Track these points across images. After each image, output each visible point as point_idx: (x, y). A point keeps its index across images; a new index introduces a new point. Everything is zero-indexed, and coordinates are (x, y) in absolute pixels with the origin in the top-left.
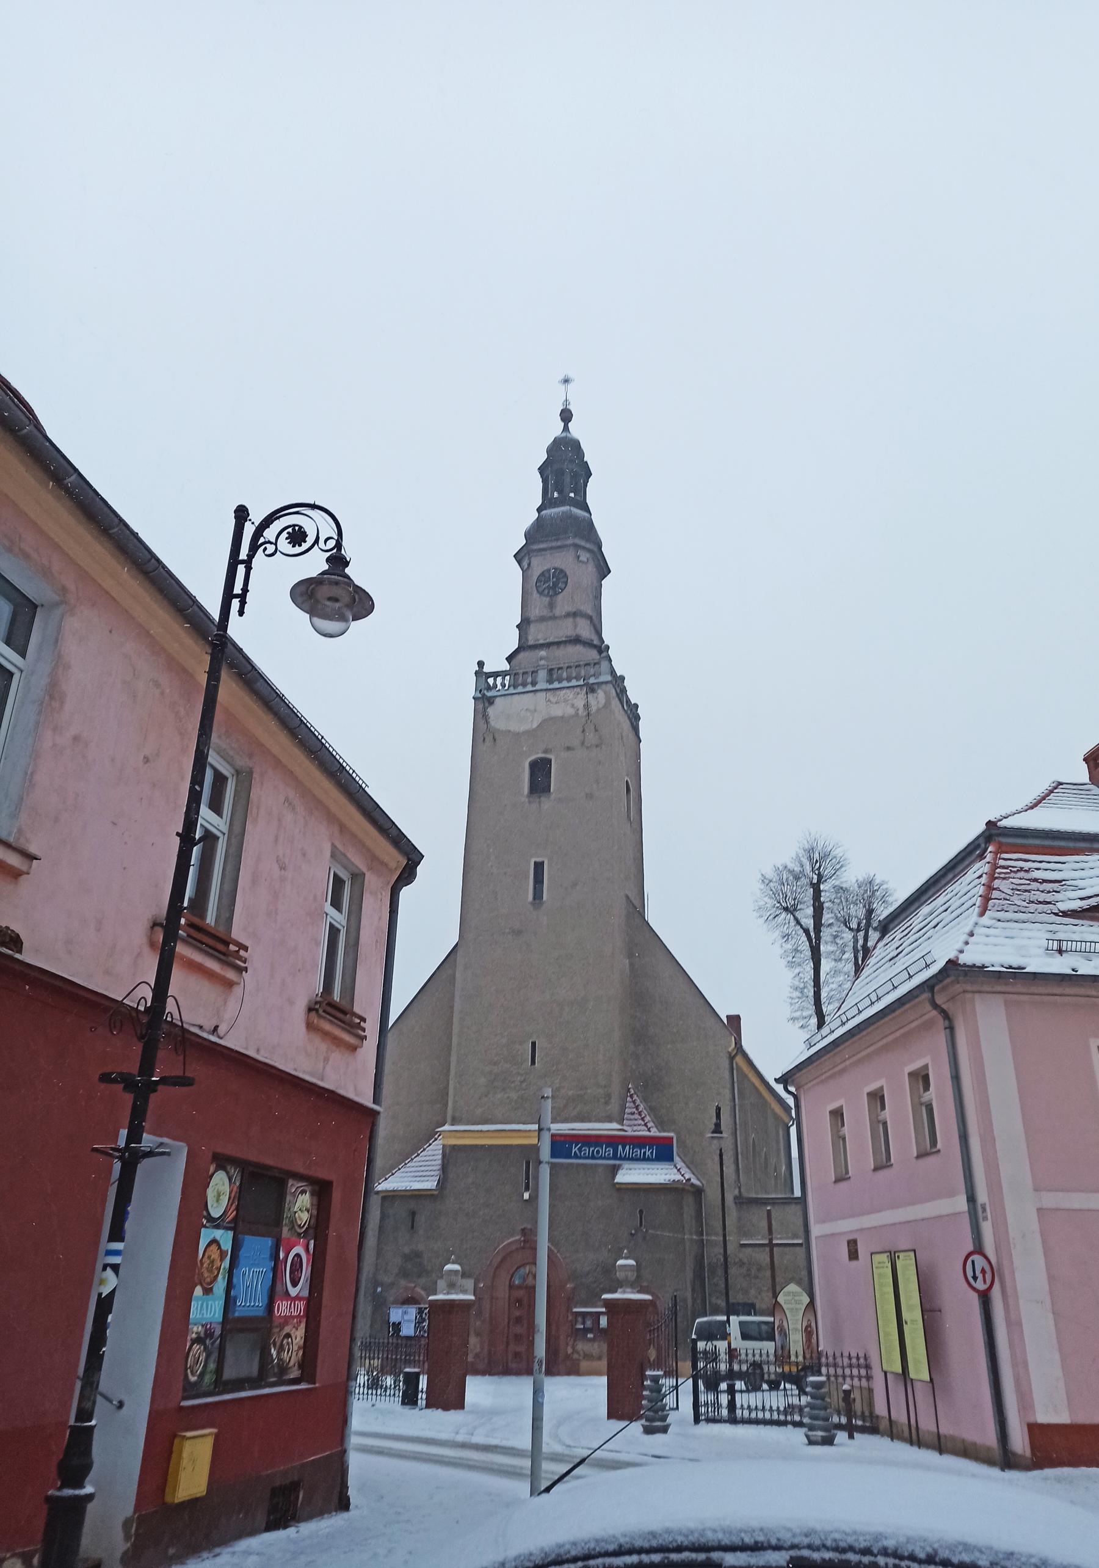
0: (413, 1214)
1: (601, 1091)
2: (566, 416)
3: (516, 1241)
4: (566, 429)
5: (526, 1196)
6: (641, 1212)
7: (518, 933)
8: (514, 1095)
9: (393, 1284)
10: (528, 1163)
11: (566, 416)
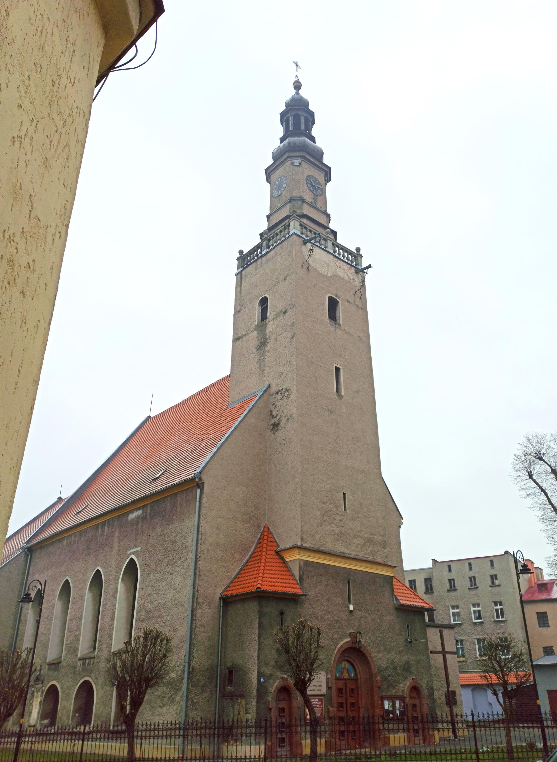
0: (282, 613)
1: (381, 538)
2: (297, 86)
3: (347, 642)
4: (297, 93)
5: (351, 607)
6: (408, 626)
7: (331, 411)
8: (337, 530)
9: (271, 675)
10: (349, 582)
11: (297, 86)
